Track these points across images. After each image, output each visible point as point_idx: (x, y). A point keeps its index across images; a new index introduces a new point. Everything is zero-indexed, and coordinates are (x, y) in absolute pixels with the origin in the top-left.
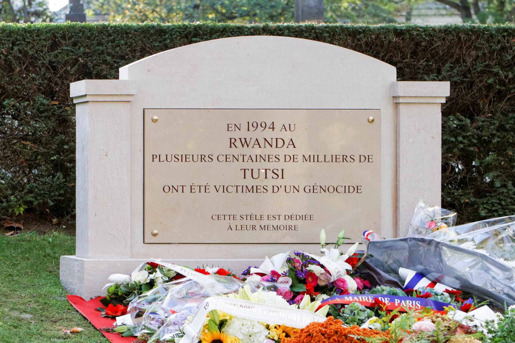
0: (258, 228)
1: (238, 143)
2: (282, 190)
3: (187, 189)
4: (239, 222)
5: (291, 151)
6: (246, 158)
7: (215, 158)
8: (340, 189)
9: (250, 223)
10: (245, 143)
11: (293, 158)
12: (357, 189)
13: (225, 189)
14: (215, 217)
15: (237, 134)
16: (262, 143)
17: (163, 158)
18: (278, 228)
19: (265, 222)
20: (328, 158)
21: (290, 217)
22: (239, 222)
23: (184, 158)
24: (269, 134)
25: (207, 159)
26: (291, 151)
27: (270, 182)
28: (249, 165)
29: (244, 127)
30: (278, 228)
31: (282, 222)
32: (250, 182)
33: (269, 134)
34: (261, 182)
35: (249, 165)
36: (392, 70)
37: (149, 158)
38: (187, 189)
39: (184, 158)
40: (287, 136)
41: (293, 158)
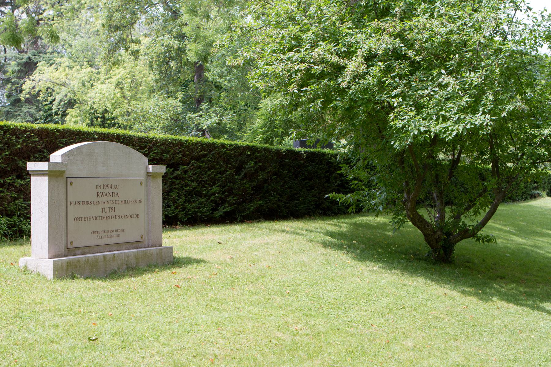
0: (107, 237)
1: (100, 195)
2: (114, 217)
3: (83, 219)
4: (101, 235)
5: (116, 198)
6: (103, 202)
7: (92, 203)
8: (133, 216)
9: (104, 234)
10: (102, 195)
11: (118, 202)
12: (137, 216)
13: (96, 218)
14: (93, 233)
15: (100, 191)
16: (108, 194)
17: (74, 203)
18: (113, 236)
19: (109, 234)
20: (129, 202)
21: (117, 231)
22: (101, 235)
23: (81, 203)
24: (110, 190)
25: (90, 203)
26: (116, 198)
27: (110, 214)
28: (104, 206)
29: (102, 187)
30: (113, 236)
31: (114, 233)
32: (104, 214)
33: (110, 190)
34: (108, 214)
35: (104, 206)
36: (146, 160)
37: (69, 203)
38: (83, 219)
39: (81, 203)
40: (115, 191)
41: (118, 202)
